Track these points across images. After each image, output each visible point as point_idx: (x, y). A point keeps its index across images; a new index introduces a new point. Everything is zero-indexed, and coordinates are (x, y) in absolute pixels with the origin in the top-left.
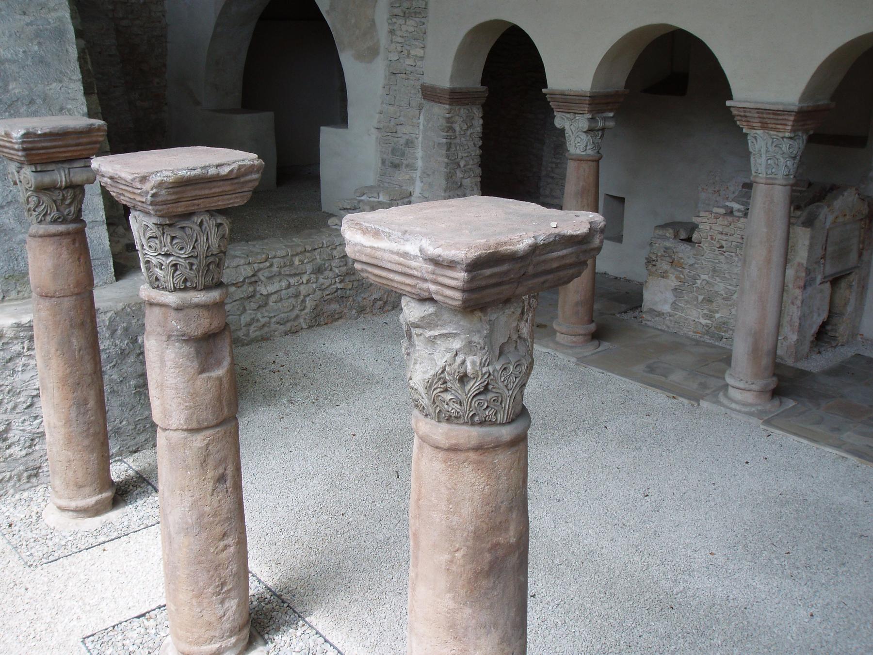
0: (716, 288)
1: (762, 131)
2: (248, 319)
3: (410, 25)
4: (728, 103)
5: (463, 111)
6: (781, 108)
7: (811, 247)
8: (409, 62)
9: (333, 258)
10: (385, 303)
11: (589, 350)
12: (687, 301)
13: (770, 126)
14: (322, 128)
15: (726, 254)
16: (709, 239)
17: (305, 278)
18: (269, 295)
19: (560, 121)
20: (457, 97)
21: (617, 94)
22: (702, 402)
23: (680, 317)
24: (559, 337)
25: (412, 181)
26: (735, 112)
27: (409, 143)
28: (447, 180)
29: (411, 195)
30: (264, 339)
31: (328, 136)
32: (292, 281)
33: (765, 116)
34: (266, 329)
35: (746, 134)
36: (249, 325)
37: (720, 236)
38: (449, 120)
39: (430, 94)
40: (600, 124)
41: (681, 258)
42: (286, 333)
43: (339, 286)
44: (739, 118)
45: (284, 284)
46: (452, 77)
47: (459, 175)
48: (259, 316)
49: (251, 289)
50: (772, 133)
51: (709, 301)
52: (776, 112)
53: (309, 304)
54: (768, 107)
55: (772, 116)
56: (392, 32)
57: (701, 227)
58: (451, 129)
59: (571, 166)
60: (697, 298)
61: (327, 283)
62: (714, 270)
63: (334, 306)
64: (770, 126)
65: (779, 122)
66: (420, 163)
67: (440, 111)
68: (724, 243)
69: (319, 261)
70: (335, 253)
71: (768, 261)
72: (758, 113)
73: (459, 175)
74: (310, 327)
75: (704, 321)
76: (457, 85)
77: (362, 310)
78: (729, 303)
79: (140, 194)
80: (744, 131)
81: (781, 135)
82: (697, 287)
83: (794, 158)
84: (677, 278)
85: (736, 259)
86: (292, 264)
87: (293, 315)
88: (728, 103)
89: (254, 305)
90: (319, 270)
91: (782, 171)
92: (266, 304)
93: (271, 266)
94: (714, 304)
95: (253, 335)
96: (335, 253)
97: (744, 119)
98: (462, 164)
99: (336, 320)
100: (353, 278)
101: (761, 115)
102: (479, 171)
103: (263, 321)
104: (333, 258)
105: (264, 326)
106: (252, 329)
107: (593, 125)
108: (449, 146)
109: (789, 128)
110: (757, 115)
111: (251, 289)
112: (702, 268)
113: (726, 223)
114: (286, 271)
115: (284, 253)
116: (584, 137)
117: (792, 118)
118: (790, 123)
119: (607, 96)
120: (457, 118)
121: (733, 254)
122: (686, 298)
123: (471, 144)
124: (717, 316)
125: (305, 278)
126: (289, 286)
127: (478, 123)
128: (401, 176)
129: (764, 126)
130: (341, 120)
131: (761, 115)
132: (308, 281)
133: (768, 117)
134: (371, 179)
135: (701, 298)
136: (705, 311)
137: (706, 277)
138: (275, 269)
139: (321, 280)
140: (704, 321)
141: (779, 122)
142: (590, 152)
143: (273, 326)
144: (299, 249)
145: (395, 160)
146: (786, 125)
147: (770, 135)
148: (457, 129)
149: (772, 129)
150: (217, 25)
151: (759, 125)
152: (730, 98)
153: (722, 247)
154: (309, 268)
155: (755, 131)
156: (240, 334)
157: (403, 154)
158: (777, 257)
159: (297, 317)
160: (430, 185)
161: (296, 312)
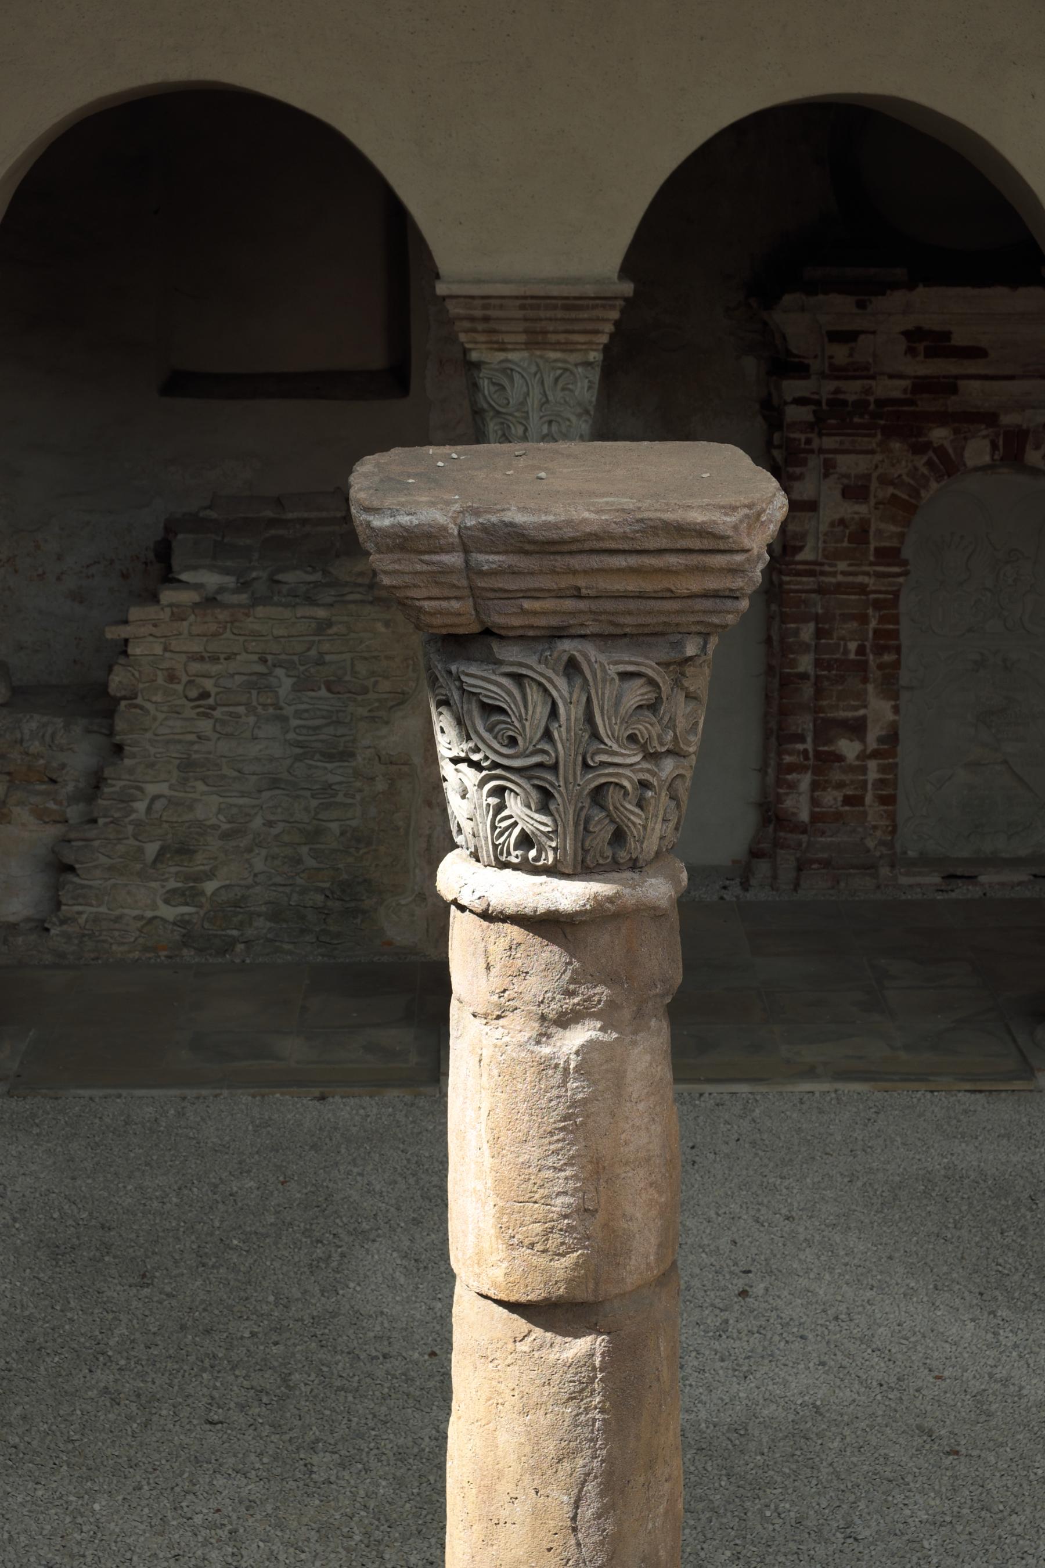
0: (199, 813)
1: (526, 354)
6: (590, 290)
12: (111, 868)
13: (553, 338)
15: (217, 714)
16: (160, 680)
23: (96, 919)
26: (454, 309)
33: (542, 314)
35: (477, 365)
37: (195, 667)
41: (38, 756)
44: (467, 324)
50: (553, 355)
51: (183, 850)
52: (572, 304)
54: (555, 291)
55: (560, 314)
57: (134, 650)
60: (141, 850)
62: (187, 765)
64: (553, 338)
65: (577, 327)
68: (208, 684)
72: (522, 307)
75: (169, 912)
78: (244, 843)
79: (734, 571)
80: (474, 356)
81: (574, 358)
82: (138, 824)
84: (41, 815)
85: (252, 720)
88: (441, 289)
94: (199, 857)
97: (480, 327)
101: (530, 313)
109: (604, 339)
110: (520, 314)
112: (152, 765)
113: (213, 627)
117: (615, 315)
118: (609, 328)
121: (241, 709)
122: (103, 860)
124: (210, 887)
129: (536, 340)
131: (530, 313)
133: (543, 315)
135: (151, 849)
136: (172, 884)
137: (163, 788)
140: (169, 912)
141: (577, 327)
146: (596, 332)
147: (547, 360)
149: (556, 346)
151: (522, 338)
153: (205, 695)
155: (502, 356)
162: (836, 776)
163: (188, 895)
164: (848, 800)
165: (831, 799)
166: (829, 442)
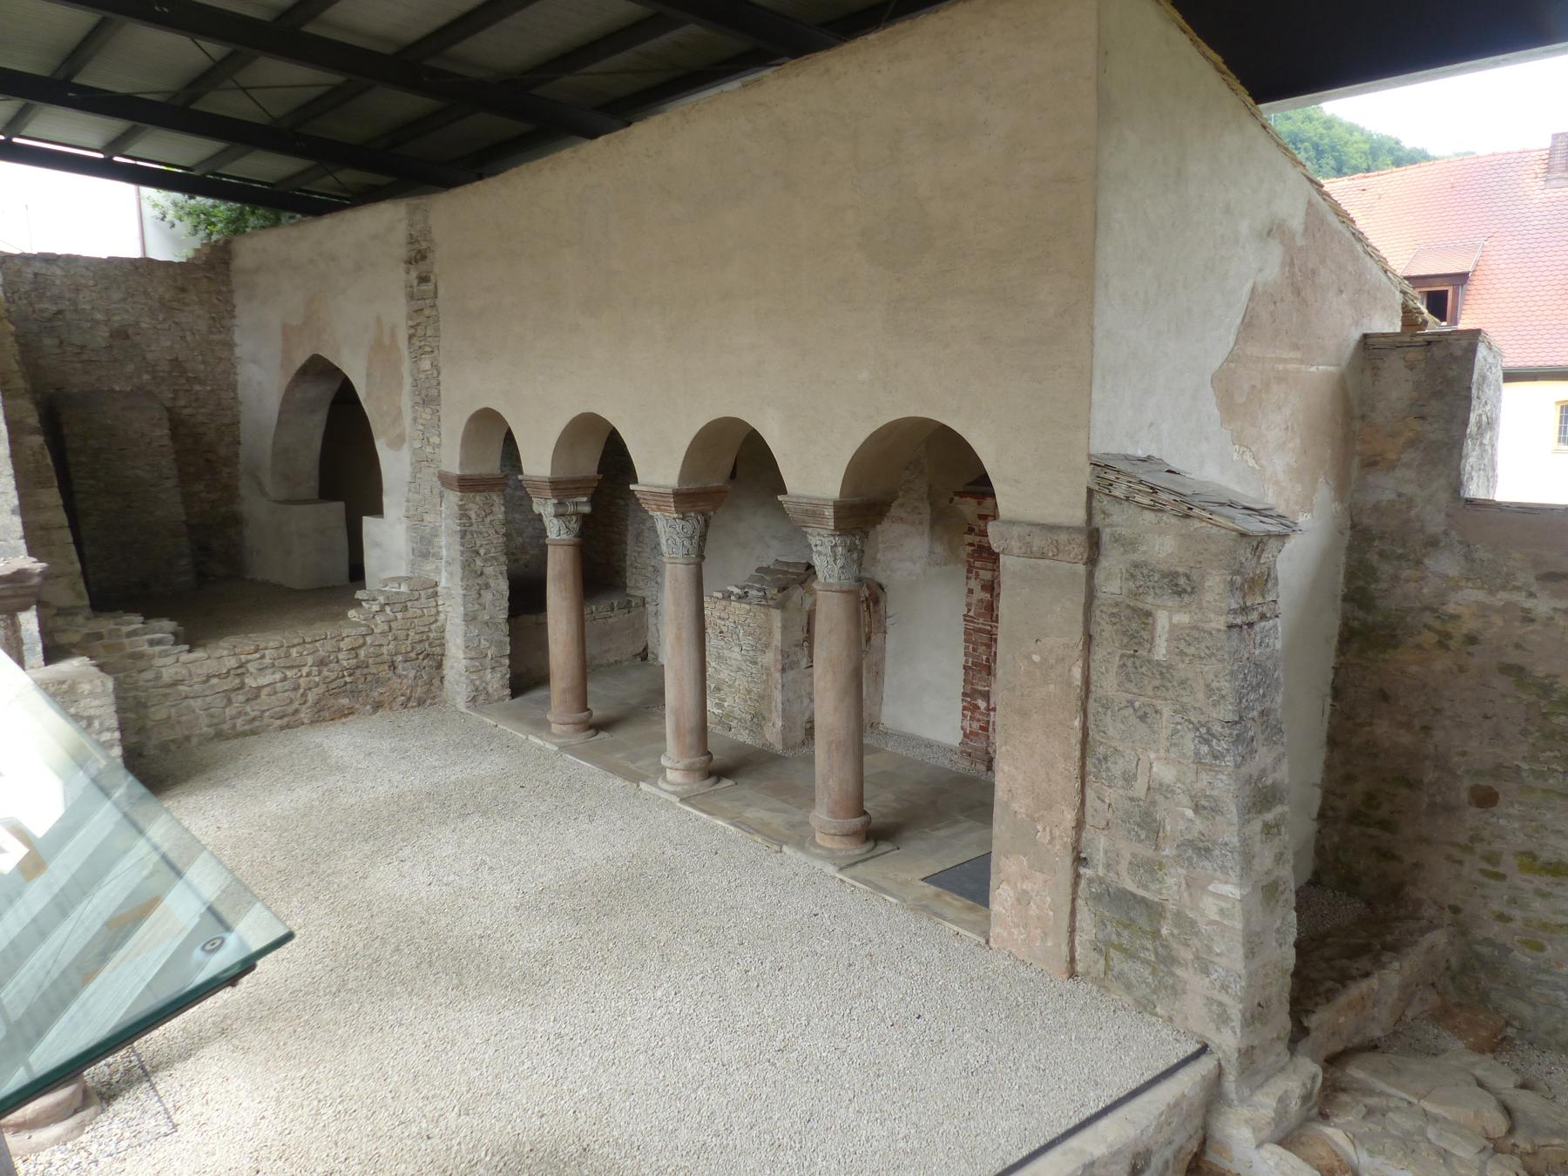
0: (722, 676)
2: (234, 712)
3: (426, 414)
4: (632, 487)
5: (479, 498)
7: (784, 628)
8: (429, 449)
9: (340, 650)
10: (409, 699)
11: (578, 739)
14: (366, 519)
17: (305, 670)
18: (259, 688)
19: (537, 508)
20: (467, 484)
21: (585, 480)
22: (643, 785)
24: (555, 728)
25: (437, 570)
27: (435, 533)
28: (463, 568)
29: (436, 585)
30: (253, 733)
31: (369, 523)
32: (289, 674)
34: (257, 723)
36: (232, 718)
38: (461, 507)
39: (444, 479)
40: (571, 509)
42: (282, 728)
43: (348, 679)
45: (278, 676)
46: (461, 464)
47: (479, 563)
48: (248, 709)
49: (237, 681)
52: (661, 495)
53: (311, 697)
56: (415, 420)
58: (464, 514)
59: (550, 549)
61: (333, 676)
63: (344, 701)
66: (444, 552)
67: (453, 497)
69: (322, 653)
70: (342, 645)
71: (678, 638)
73: (479, 563)
74: (312, 722)
76: (468, 472)
77: (377, 706)
83: (691, 538)
86: (288, 655)
87: (290, 709)
88: (632, 487)
89: (241, 698)
90: (322, 663)
91: (681, 551)
92: (257, 697)
93: (263, 657)
95: (239, 728)
96: (342, 645)
98: (482, 552)
99: (346, 716)
100: (366, 671)
102: (503, 559)
103: (253, 714)
104: (340, 650)
105: (254, 719)
106: (239, 722)
107: (561, 510)
108: (463, 534)
111: (237, 681)
114: (282, 662)
115: (276, 644)
116: (555, 521)
119: (574, 481)
120: (472, 506)
123: (491, 531)
125: (305, 670)
126: (285, 679)
127: (499, 512)
128: (429, 566)
130: (377, 511)
132: (308, 675)
134: (403, 572)
138: (267, 661)
139: (325, 673)
142: (564, 536)
143: (266, 721)
144: (296, 641)
145: (423, 549)
148: (473, 516)
150: (280, 413)
152: (635, 481)
154: (310, 660)
156: (225, 727)
157: (430, 543)
158: (688, 633)
159: (296, 711)
160: (451, 574)
161: (296, 705)
162: (977, 716)
163: (719, 706)
164: (981, 728)
165: (976, 725)
166: (977, 564)
